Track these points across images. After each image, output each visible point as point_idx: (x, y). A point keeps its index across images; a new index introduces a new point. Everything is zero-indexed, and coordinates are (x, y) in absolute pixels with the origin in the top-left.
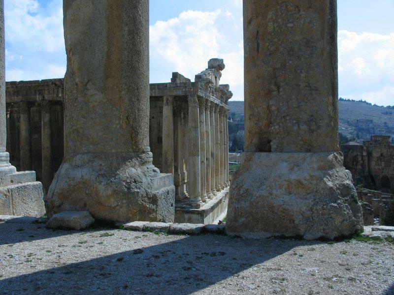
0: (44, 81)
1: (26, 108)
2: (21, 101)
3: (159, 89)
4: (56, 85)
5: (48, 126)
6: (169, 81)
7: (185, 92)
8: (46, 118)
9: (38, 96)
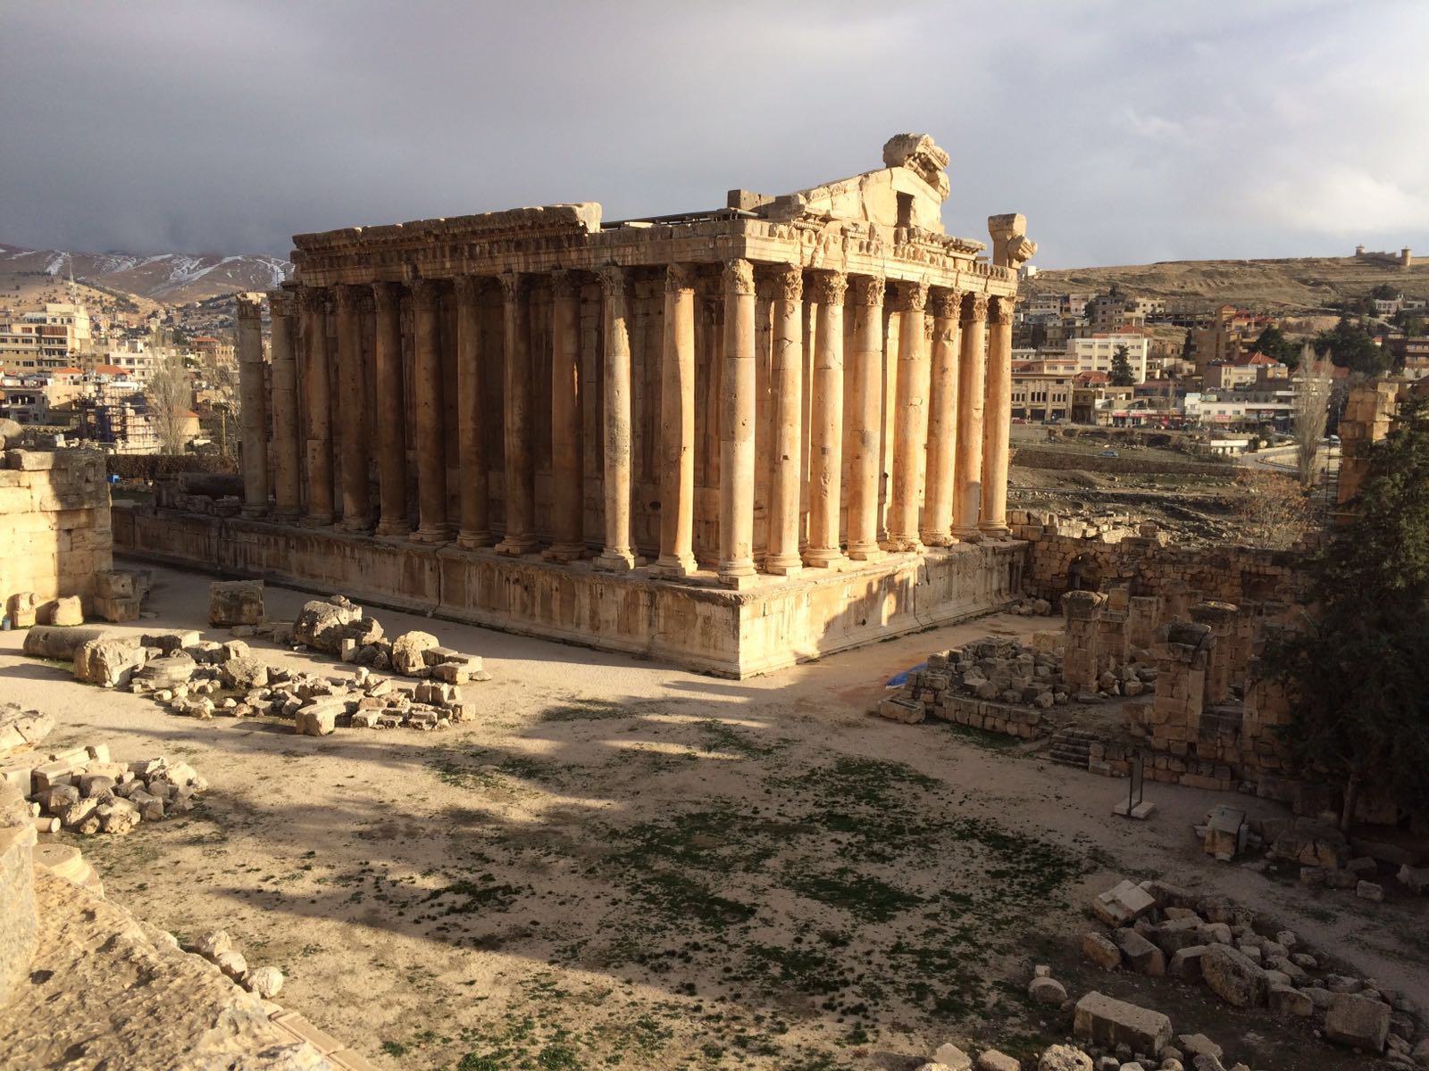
0: (408, 226)
2: (375, 281)
4: (437, 237)
8: (422, 326)
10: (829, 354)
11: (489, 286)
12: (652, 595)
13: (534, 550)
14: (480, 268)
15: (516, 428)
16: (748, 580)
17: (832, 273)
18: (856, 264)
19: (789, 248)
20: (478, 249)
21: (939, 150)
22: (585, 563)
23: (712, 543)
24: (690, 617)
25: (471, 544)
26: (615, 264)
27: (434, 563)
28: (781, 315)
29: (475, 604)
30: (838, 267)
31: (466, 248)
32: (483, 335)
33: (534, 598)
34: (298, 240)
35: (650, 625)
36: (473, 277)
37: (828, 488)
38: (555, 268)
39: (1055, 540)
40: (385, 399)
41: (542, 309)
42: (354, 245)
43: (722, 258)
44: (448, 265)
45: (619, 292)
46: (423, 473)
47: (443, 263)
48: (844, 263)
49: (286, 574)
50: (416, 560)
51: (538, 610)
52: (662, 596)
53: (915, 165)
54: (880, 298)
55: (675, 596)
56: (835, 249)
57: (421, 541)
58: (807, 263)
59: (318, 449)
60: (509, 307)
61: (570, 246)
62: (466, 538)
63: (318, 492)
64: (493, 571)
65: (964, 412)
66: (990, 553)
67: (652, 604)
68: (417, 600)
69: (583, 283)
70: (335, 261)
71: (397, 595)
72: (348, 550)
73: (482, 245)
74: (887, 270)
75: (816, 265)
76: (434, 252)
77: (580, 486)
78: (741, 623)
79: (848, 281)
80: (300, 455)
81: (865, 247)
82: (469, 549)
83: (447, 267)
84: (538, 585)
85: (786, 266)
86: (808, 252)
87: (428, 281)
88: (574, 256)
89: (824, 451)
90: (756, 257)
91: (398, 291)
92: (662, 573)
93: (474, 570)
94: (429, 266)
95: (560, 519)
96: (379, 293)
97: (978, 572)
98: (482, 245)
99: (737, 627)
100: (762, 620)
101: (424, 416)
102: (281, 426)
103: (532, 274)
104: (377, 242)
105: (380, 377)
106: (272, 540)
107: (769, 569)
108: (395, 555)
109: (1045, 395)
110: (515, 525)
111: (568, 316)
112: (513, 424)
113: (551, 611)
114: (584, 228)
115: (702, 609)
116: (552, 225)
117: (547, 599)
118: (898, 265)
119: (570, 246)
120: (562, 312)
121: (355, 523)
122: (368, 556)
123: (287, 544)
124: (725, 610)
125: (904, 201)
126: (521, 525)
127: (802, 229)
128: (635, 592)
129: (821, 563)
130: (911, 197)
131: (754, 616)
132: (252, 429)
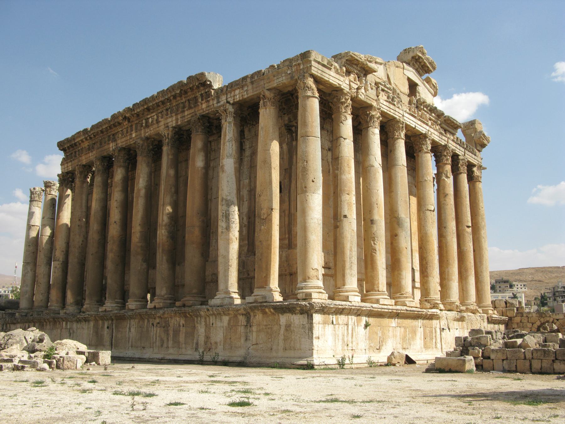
0: (114, 117)
1: (100, 167)
3: (252, 83)
8: (119, 174)
9: (111, 145)
10: (372, 158)
12: (247, 316)
13: (172, 305)
15: (164, 223)
16: (316, 290)
17: (370, 107)
18: (385, 106)
19: (342, 79)
20: (150, 120)
21: (431, 59)
23: (290, 275)
24: (275, 328)
26: (228, 102)
29: (132, 347)
30: (374, 104)
31: (144, 121)
32: (150, 175)
33: (168, 334)
34: (62, 146)
35: (246, 340)
36: (147, 138)
37: (377, 247)
38: (192, 117)
39: (525, 315)
40: (95, 226)
42: (86, 139)
44: (134, 135)
45: (230, 119)
47: (131, 134)
48: (377, 100)
50: (100, 322)
52: (255, 316)
53: (417, 66)
54: (403, 135)
55: (264, 313)
56: (372, 93)
57: (105, 311)
59: (58, 266)
60: (165, 149)
61: (202, 100)
62: (132, 304)
63: (54, 294)
65: (460, 228)
66: (486, 320)
67: (249, 324)
70: (77, 153)
72: (64, 323)
78: (314, 325)
82: (133, 310)
83: (133, 137)
84: (171, 325)
85: (338, 90)
88: (204, 106)
89: (372, 222)
90: (319, 75)
93: (133, 322)
94: (123, 140)
99: (311, 329)
100: (331, 326)
101: (114, 230)
113: (179, 342)
114: (210, 86)
115: (283, 319)
116: (192, 89)
117: (176, 333)
119: (202, 100)
121: (71, 309)
122: (75, 325)
124: (301, 316)
125: (413, 86)
126: (164, 289)
129: (374, 301)
131: (325, 323)
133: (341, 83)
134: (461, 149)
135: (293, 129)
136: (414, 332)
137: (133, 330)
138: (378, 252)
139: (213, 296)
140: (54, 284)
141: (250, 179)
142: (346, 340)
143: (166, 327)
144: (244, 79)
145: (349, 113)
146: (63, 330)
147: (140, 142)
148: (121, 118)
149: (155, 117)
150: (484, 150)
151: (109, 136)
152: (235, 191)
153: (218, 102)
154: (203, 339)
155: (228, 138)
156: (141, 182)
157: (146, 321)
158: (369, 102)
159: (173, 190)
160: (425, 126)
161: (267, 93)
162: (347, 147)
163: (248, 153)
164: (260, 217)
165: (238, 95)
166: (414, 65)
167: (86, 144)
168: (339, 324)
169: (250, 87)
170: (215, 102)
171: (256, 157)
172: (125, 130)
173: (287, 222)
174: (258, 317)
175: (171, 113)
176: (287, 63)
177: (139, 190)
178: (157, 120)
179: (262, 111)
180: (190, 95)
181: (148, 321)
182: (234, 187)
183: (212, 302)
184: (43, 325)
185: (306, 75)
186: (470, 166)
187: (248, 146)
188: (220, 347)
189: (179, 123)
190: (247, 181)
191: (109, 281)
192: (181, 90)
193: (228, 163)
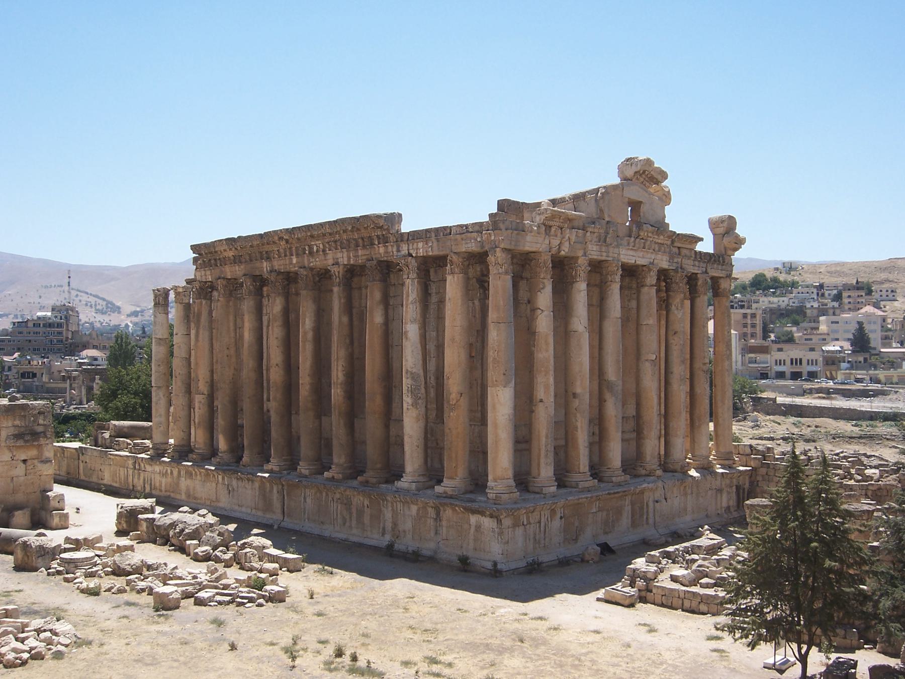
2: (245, 275)
3: (438, 241)
4: (287, 241)
5: (279, 323)
6: (487, 219)
7: (482, 244)
9: (265, 264)
11: (324, 275)
13: (353, 477)
14: (317, 262)
15: (340, 381)
18: (595, 252)
22: (389, 486)
24: (466, 526)
25: (306, 472)
26: (410, 255)
27: (280, 487)
28: (533, 290)
30: (580, 253)
33: (351, 514)
34: (195, 248)
35: (436, 533)
36: (312, 269)
37: (579, 424)
39: (771, 467)
40: (249, 363)
41: (364, 290)
42: (231, 250)
43: (486, 248)
44: (294, 261)
45: (413, 275)
46: (274, 417)
49: (178, 497)
51: (354, 523)
52: (445, 511)
54: (618, 278)
55: (454, 510)
58: (554, 251)
59: (203, 401)
60: (336, 289)
62: (304, 468)
64: (321, 493)
67: (438, 518)
68: (268, 516)
69: (388, 270)
71: (254, 511)
72: (220, 477)
73: (317, 245)
74: (622, 256)
75: (563, 253)
76: (285, 252)
77: (387, 426)
79: (590, 265)
80: (190, 406)
81: (602, 240)
82: (306, 477)
86: (555, 242)
87: (279, 273)
90: (512, 247)
91: (260, 282)
92: (445, 492)
95: (372, 451)
96: (248, 284)
97: (710, 493)
98: (317, 245)
100: (522, 528)
101: (275, 375)
102: (177, 385)
103: (353, 265)
104: (245, 247)
105: (246, 345)
106: (169, 471)
107: (531, 489)
108: (253, 481)
109: (801, 360)
110: (339, 458)
111: (378, 295)
112: (338, 378)
114: (388, 230)
115: (474, 519)
117: (360, 513)
118: (631, 253)
120: (373, 294)
123: (179, 472)
127: (550, 227)
128: (424, 508)
129: (574, 484)
130: (641, 202)
131: (515, 525)
132: (159, 388)
133: (539, 246)
134: (702, 264)
135: (486, 284)
136: (619, 512)
137: (309, 500)
138: (579, 430)
139: (399, 476)
140: (199, 423)
141: (438, 331)
142: (537, 538)
143: (348, 504)
144: (428, 231)
145: (549, 277)
146: (220, 486)
147: (303, 272)
148: (276, 238)
149: (321, 246)
150: (736, 253)
151: (261, 253)
152: (421, 362)
153: (398, 251)
154: (390, 525)
155: (411, 299)
156: (307, 323)
157: (324, 494)
158: (573, 255)
159: (348, 341)
160: (649, 255)
161: (455, 258)
162: (544, 323)
163: (434, 299)
164: (448, 402)
165: (421, 249)
166: (637, 179)
167: (230, 254)
168: (529, 523)
169: (435, 244)
170: (395, 250)
171: (444, 306)
172: (281, 250)
173: (479, 393)
174: (448, 513)
175: (342, 248)
176: (477, 228)
177: (305, 333)
178: (324, 251)
179: (449, 278)
180: (365, 234)
181: (327, 495)
182: (420, 357)
183: (400, 484)
184: (191, 474)
185: (498, 249)
186: (715, 281)
187: (434, 291)
188: (409, 536)
189: (352, 262)
190: (434, 334)
191: (274, 434)
192: (353, 227)
193: (412, 330)
